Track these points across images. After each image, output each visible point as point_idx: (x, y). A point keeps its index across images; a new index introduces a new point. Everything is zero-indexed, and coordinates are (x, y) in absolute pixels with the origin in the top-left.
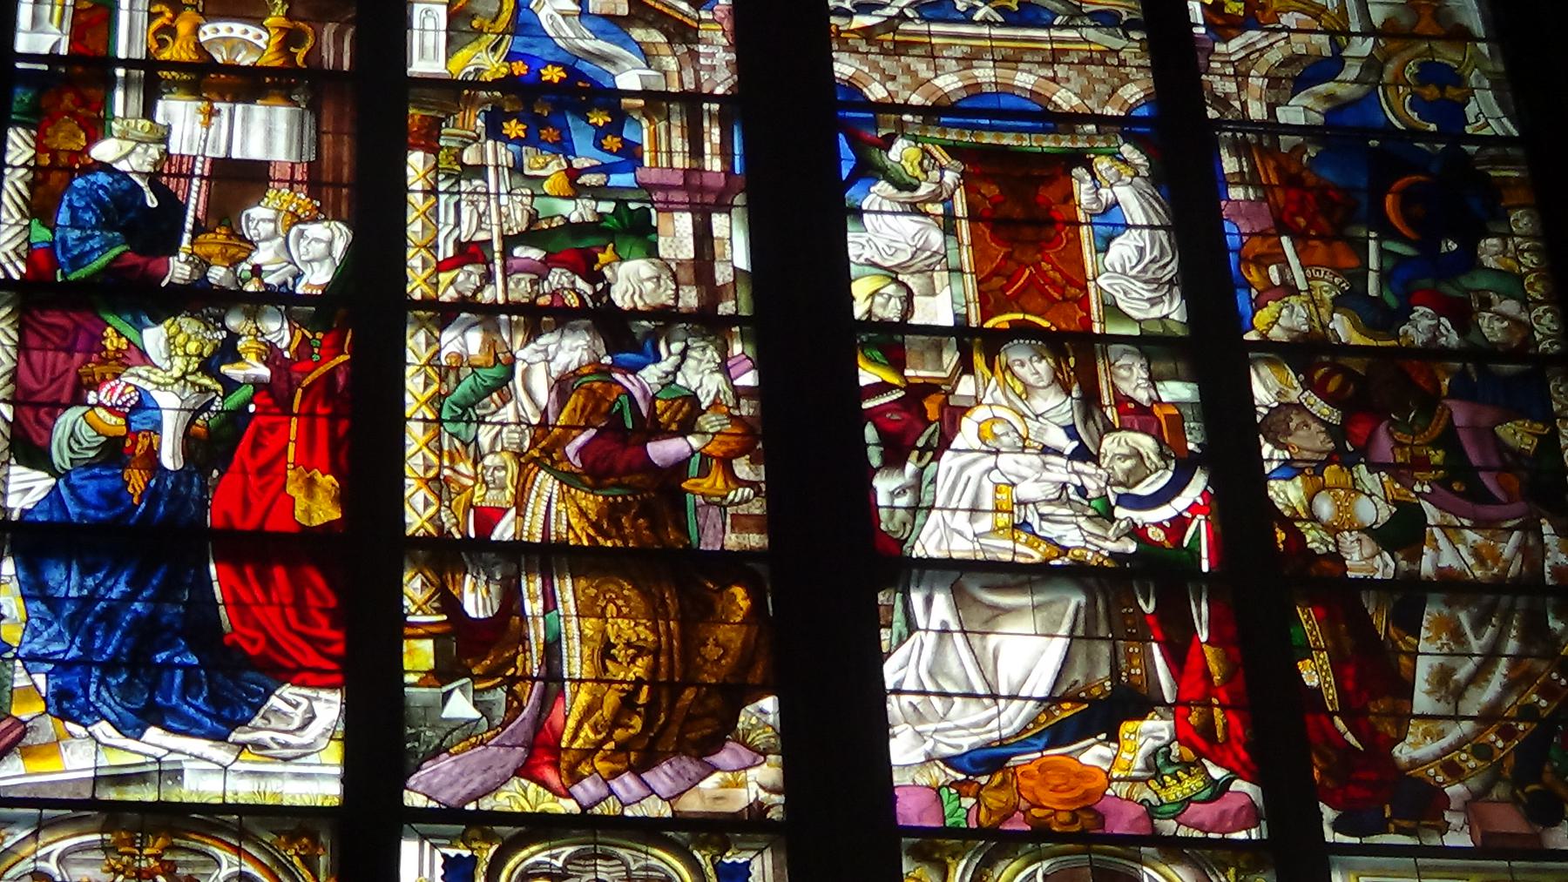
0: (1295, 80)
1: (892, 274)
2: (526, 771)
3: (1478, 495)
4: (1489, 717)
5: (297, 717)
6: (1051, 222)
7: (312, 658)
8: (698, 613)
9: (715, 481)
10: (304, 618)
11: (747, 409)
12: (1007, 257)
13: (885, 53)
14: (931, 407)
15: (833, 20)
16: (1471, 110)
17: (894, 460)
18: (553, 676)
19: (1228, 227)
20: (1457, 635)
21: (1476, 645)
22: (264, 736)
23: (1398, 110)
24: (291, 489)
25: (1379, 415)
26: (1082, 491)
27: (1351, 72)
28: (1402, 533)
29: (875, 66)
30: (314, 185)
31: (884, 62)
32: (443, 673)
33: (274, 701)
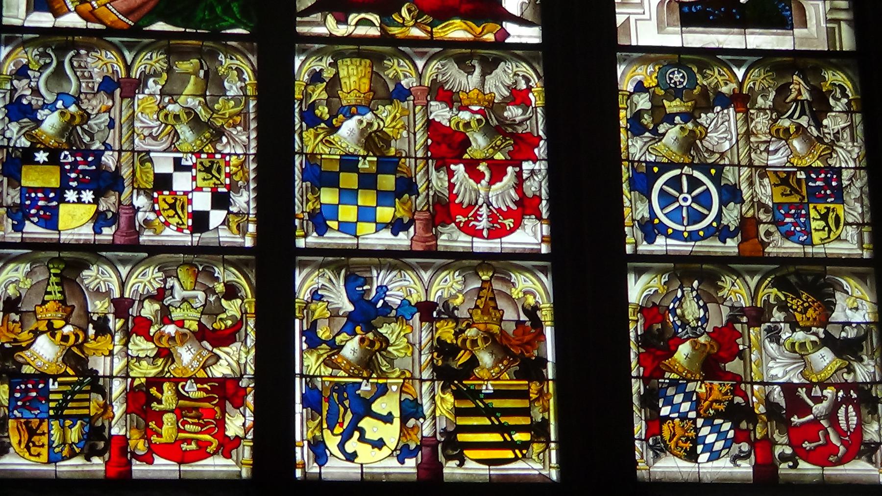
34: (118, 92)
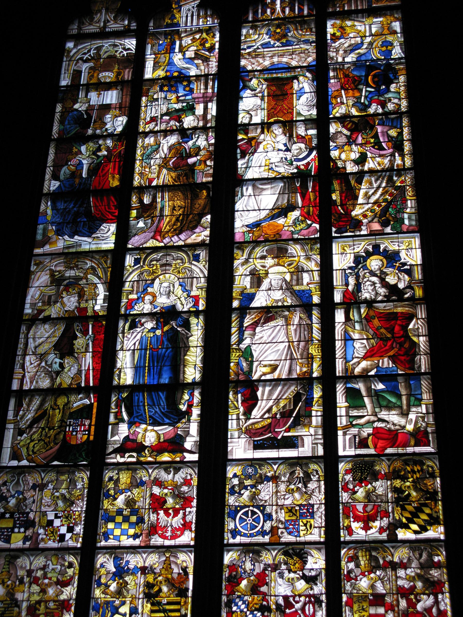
1: (248, 112)
13: (253, 58)
14: (253, 143)
17: (243, 156)
29: (250, 62)
31: (252, 60)
34: (37, 489)
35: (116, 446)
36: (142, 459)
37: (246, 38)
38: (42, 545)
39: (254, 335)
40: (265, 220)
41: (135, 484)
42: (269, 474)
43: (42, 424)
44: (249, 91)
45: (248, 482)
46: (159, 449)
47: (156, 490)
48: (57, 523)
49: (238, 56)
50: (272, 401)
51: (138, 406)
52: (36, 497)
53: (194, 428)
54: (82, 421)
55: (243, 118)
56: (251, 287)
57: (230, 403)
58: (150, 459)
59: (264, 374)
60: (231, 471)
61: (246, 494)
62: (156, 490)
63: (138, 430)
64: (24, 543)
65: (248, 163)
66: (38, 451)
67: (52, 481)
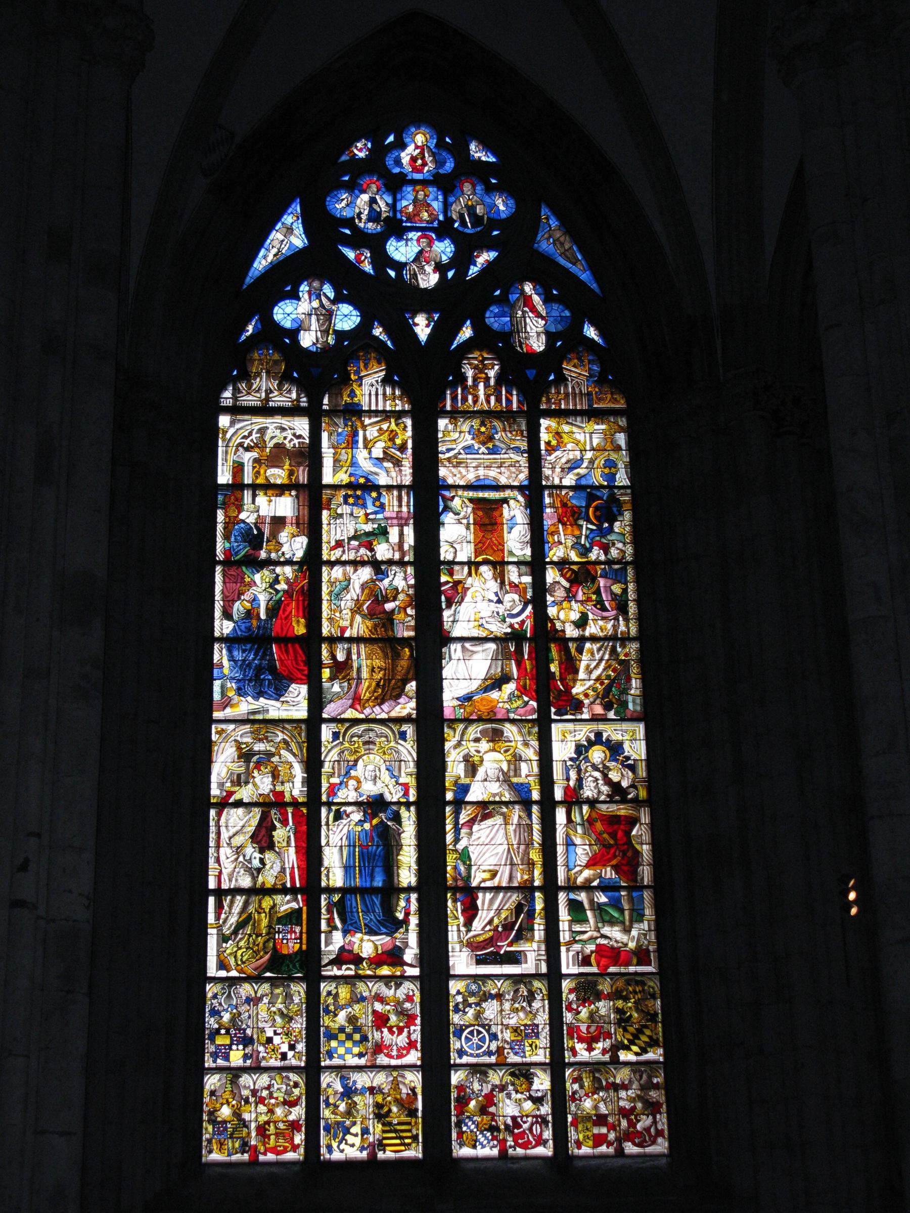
0: (569, 468)
2: (352, 706)
3: (604, 609)
4: (597, 680)
5: (296, 693)
6: (496, 524)
7: (300, 676)
8: (396, 656)
9: (402, 615)
10: (297, 664)
11: (411, 592)
12: (483, 536)
14: (460, 588)
15: (440, 455)
16: (618, 476)
17: (449, 606)
18: (359, 678)
19: (545, 523)
20: (592, 654)
21: (597, 657)
22: (288, 699)
23: (597, 478)
24: (294, 624)
25: (580, 584)
26: (498, 613)
27: (585, 465)
28: (582, 623)
30: (298, 524)
31: (454, 470)
32: (331, 679)
33: (290, 689)
35: (332, 957)
36: (360, 972)
37: (444, 435)
38: (264, 1064)
39: (470, 834)
40: (476, 692)
41: (355, 999)
42: (493, 992)
43: (249, 930)
44: (451, 515)
45: (471, 1000)
46: (378, 961)
47: (378, 1007)
48: (277, 1040)
49: (435, 463)
50: (493, 912)
51: (352, 912)
52: (251, 1012)
53: (413, 938)
54: (292, 928)
55: (446, 553)
56: (465, 777)
57: (449, 912)
58: (369, 972)
59: (484, 881)
60: (454, 986)
61: (471, 1012)
62: (378, 1007)
63: (353, 939)
64: (245, 1062)
65: (454, 615)
66: (247, 960)
67: (267, 995)
